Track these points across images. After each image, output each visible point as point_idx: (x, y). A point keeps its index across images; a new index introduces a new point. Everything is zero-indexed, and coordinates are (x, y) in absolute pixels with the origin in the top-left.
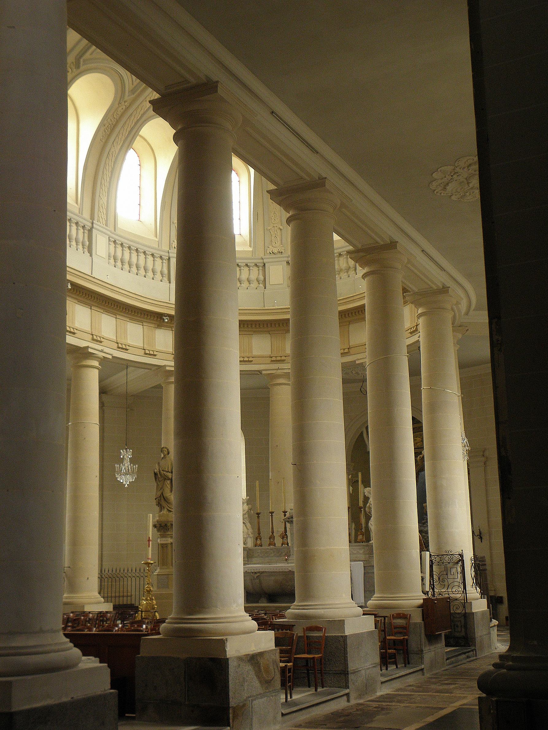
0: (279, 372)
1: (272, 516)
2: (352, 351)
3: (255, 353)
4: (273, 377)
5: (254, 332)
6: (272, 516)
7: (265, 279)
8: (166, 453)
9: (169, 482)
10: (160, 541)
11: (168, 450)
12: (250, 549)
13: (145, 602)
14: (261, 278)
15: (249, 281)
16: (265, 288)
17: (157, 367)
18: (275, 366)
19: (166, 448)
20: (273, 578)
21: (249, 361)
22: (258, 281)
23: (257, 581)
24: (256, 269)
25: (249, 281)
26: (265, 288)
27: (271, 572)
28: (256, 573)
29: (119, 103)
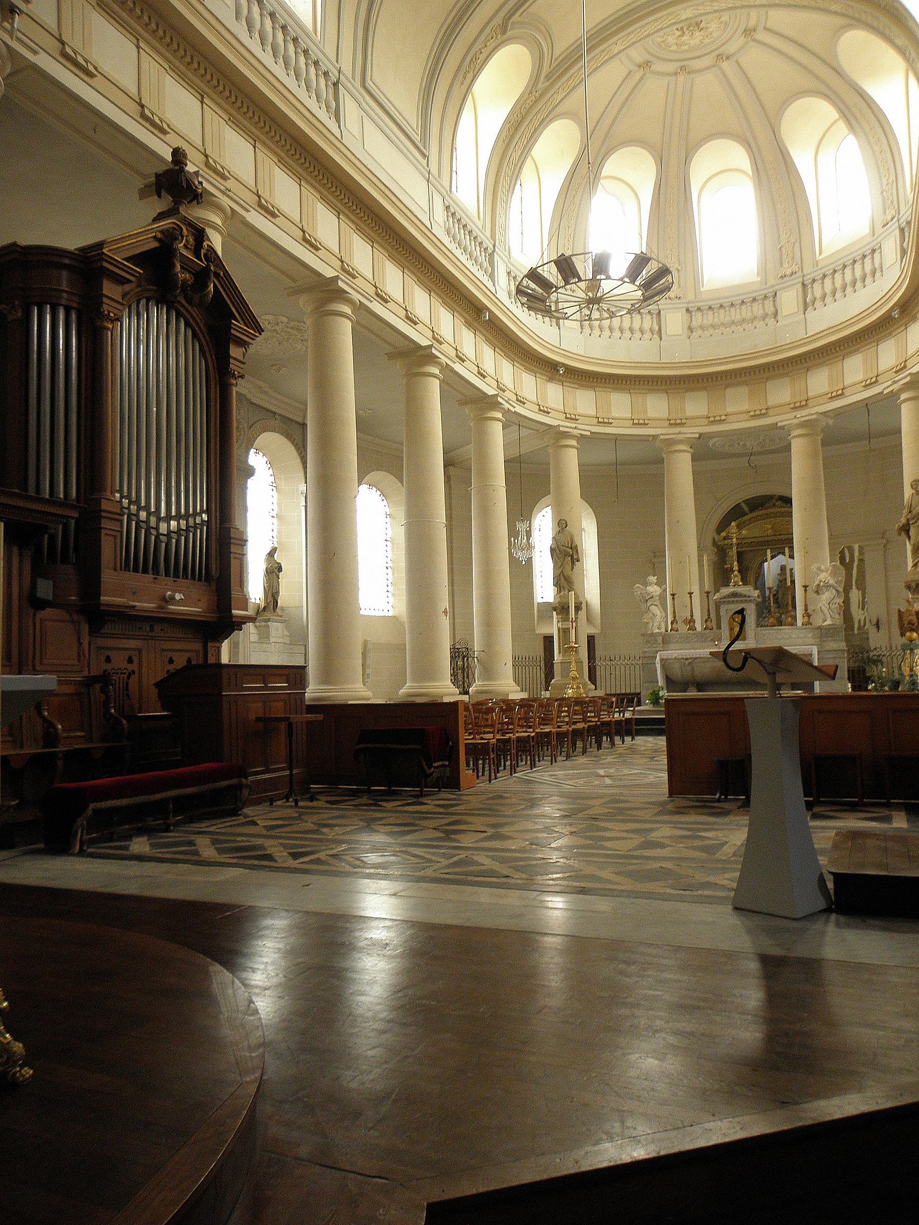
0: (680, 437)
1: (691, 597)
2: (771, 412)
3: (651, 414)
4: (671, 442)
5: (650, 390)
6: (691, 597)
7: (660, 329)
8: (564, 526)
9: (569, 558)
10: (562, 624)
11: (566, 523)
13: (571, 691)
14: (657, 328)
15: (642, 331)
16: (661, 340)
17: (547, 428)
18: (677, 430)
19: (564, 520)
20: (709, 665)
21: (645, 424)
22: (651, 330)
23: (689, 668)
24: (649, 317)
25: (642, 331)
26: (661, 340)
28: (687, 659)
29: (531, 93)
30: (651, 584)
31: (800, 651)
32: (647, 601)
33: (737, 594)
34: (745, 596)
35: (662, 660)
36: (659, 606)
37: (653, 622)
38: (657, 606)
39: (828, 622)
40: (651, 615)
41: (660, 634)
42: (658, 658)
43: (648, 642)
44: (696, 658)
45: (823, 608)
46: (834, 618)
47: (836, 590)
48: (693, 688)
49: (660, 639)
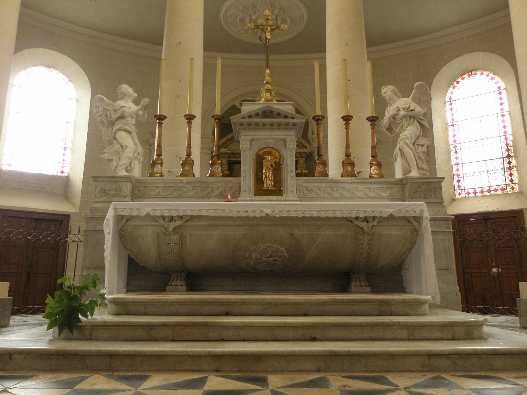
12: (138, 181)
20: (216, 232)
27: (214, 218)
30: (124, 95)
31: (400, 211)
32: (114, 124)
33: (271, 112)
34: (286, 117)
35: (119, 218)
36: (134, 134)
37: (119, 159)
38: (130, 132)
39: (414, 173)
40: (117, 147)
41: (128, 179)
42: (110, 215)
43: (103, 192)
44: (192, 218)
45: (407, 150)
46: (422, 169)
47: (421, 125)
48: (179, 282)
49: (127, 188)
